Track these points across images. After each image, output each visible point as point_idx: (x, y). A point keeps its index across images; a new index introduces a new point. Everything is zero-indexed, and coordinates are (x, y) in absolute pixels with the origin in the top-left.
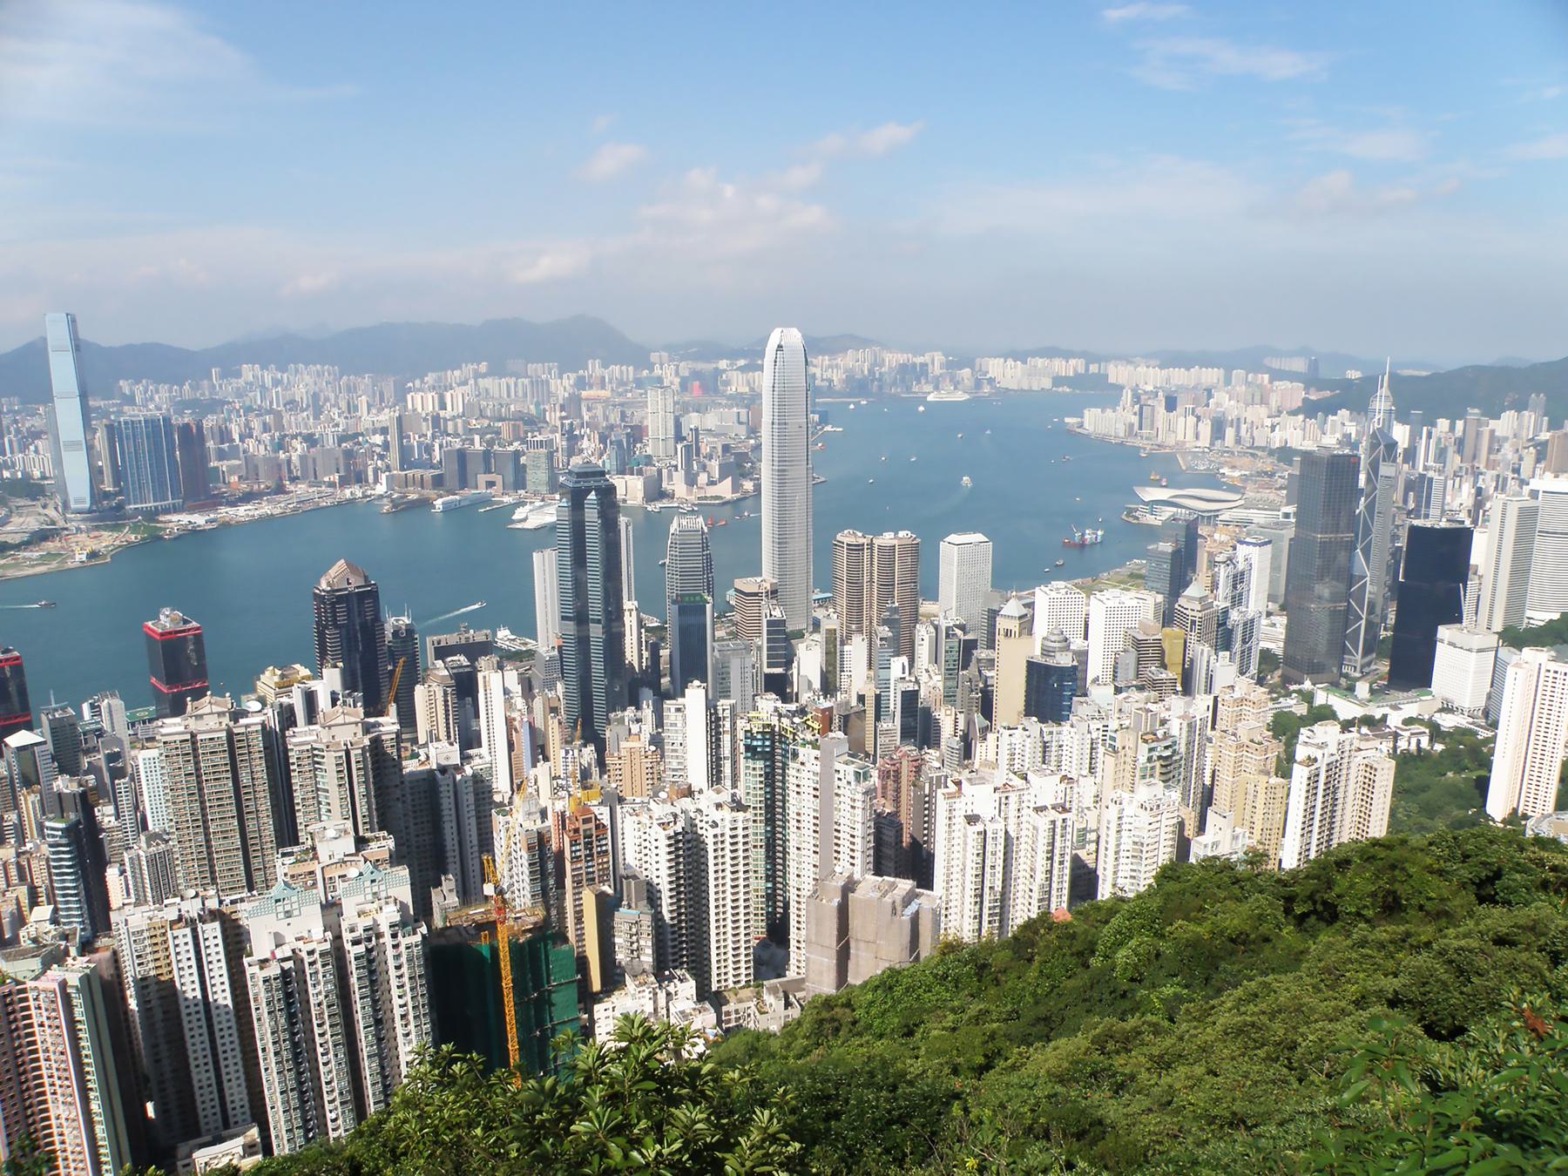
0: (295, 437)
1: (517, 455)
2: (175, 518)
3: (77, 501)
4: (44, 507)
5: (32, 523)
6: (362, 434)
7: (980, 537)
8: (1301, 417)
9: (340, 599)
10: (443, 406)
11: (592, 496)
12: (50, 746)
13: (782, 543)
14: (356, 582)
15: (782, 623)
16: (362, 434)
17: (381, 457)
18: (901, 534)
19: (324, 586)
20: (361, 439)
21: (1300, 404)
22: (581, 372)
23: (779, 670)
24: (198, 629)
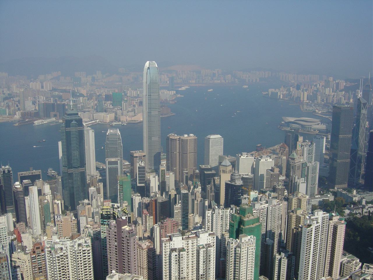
7: (219, 136)
8: (344, 92)
10: (42, 87)
13: (150, 138)
15: (144, 168)
18: (191, 135)
20: (12, 99)
21: (343, 88)
22: (94, 76)
23: (143, 185)
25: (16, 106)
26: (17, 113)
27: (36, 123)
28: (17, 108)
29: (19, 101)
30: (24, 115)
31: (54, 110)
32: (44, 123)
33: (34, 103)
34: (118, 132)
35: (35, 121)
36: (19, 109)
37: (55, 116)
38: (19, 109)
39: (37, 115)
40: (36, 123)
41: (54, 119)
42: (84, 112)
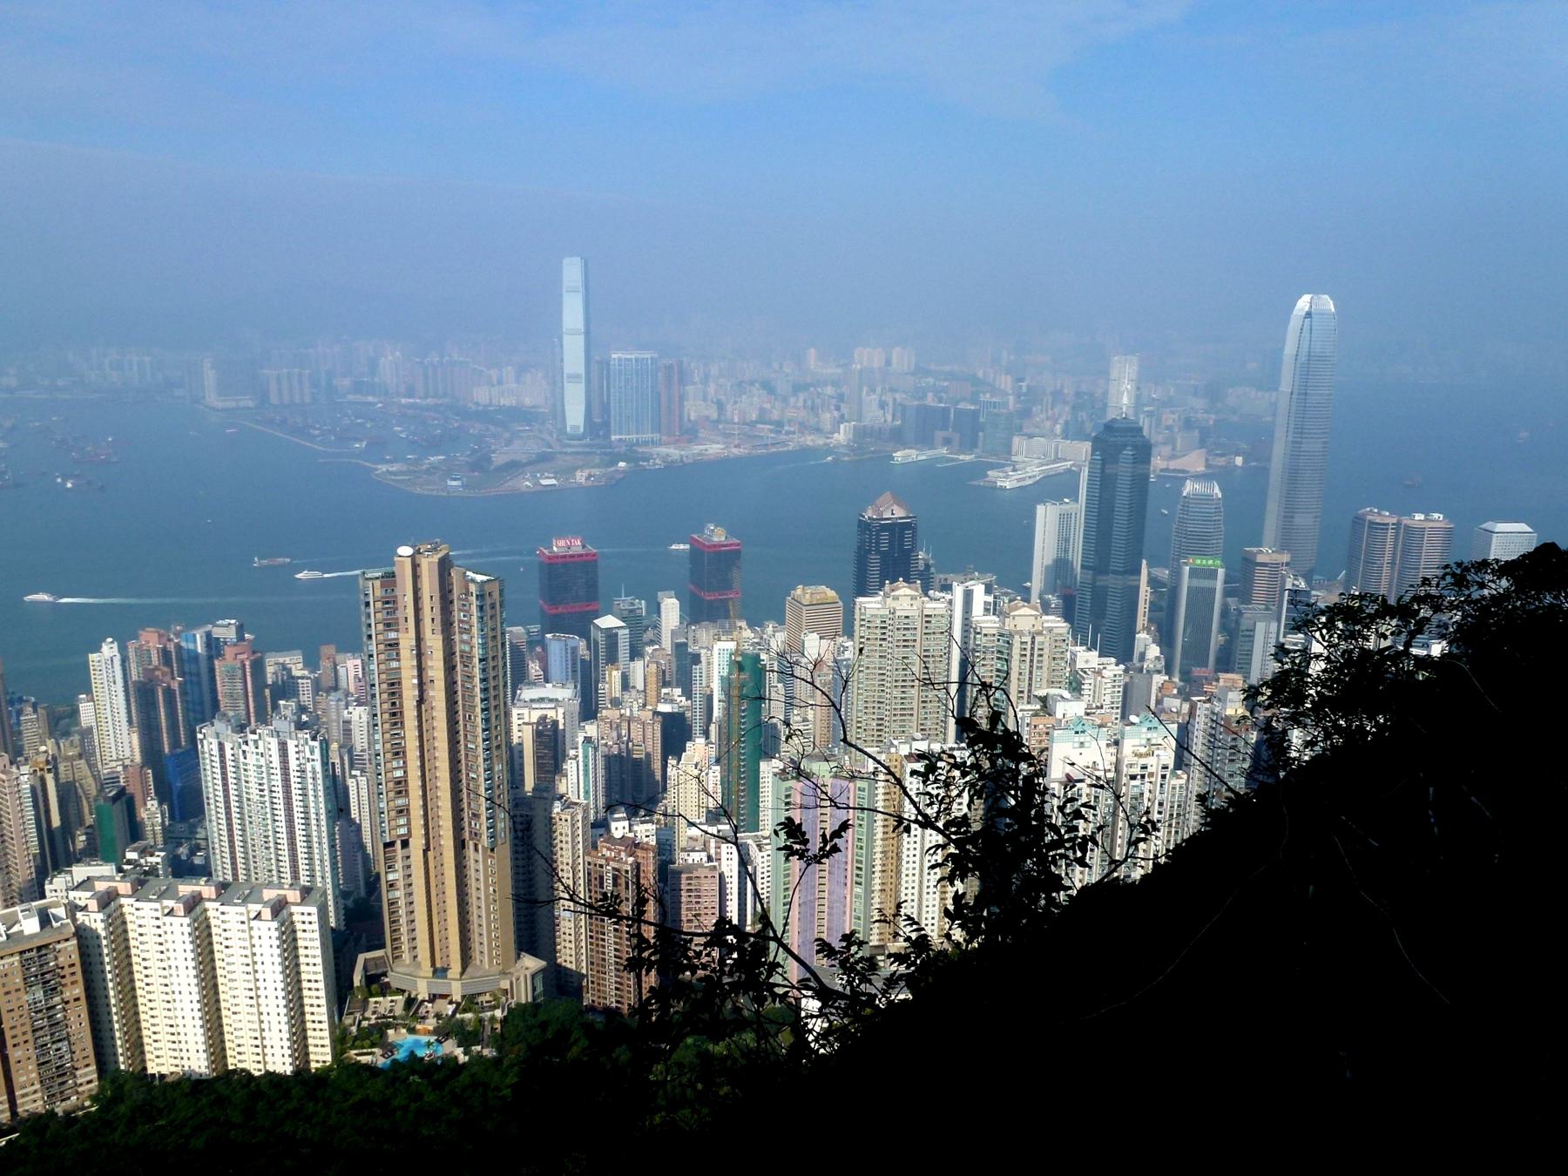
0: (752, 383)
1: (975, 414)
2: (663, 450)
3: (573, 427)
4: (540, 431)
5: (534, 448)
6: (813, 385)
9: (884, 528)
10: (888, 362)
11: (1128, 452)
12: (627, 631)
14: (899, 513)
16: (813, 385)
17: (838, 408)
19: (869, 514)
24: (738, 545)
25: (833, 408)
26: (842, 426)
27: (899, 456)
28: (836, 414)
29: (841, 398)
30: (861, 434)
31: (945, 427)
32: (920, 458)
33: (882, 406)
34: (1217, 490)
35: (895, 452)
36: (842, 417)
37: (947, 442)
38: (842, 417)
39: (898, 437)
40: (899, 456)
41: (943, 451)
42: (1030, 436)
